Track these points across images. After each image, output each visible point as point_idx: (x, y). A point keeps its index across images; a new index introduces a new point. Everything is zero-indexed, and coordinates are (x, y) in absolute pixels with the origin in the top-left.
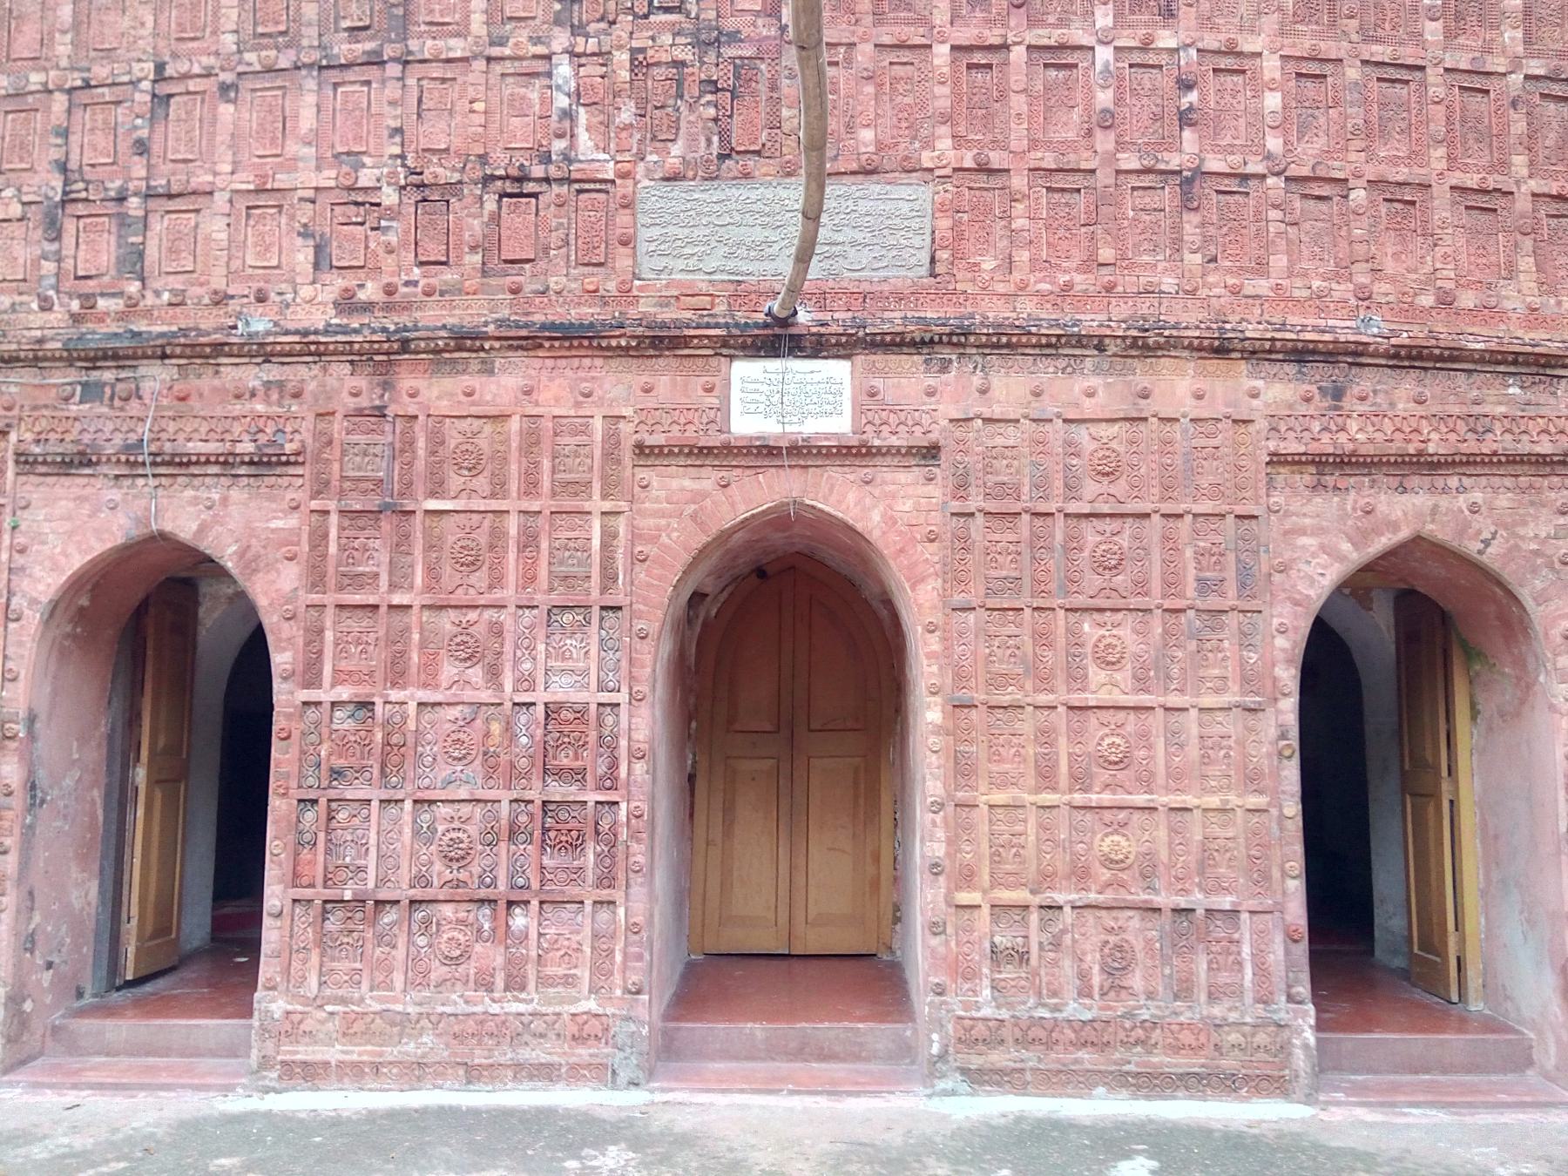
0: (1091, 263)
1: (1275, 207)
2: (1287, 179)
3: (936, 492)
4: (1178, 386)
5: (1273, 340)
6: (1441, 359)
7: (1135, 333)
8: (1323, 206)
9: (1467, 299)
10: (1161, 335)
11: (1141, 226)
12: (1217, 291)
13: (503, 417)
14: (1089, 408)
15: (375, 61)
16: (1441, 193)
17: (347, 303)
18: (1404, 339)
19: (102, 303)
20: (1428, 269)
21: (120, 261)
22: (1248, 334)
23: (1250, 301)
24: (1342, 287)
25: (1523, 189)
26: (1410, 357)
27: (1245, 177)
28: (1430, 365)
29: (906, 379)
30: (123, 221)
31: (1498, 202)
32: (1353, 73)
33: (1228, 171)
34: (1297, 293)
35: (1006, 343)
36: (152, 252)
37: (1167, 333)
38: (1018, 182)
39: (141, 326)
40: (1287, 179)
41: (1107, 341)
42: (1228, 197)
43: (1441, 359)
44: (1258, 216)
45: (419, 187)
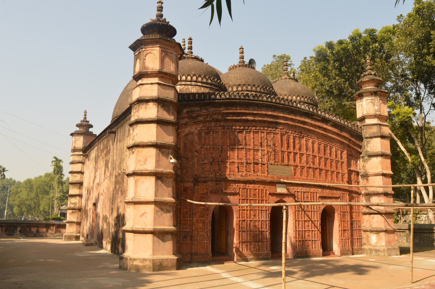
13: (256, 189)
14: (305, 191)
17: (242, 176)
19: (217, 174)
21: (219, 169)
36: (222, 169)
38: (299, 167)
39: (222, 177)
45: (247, 163)
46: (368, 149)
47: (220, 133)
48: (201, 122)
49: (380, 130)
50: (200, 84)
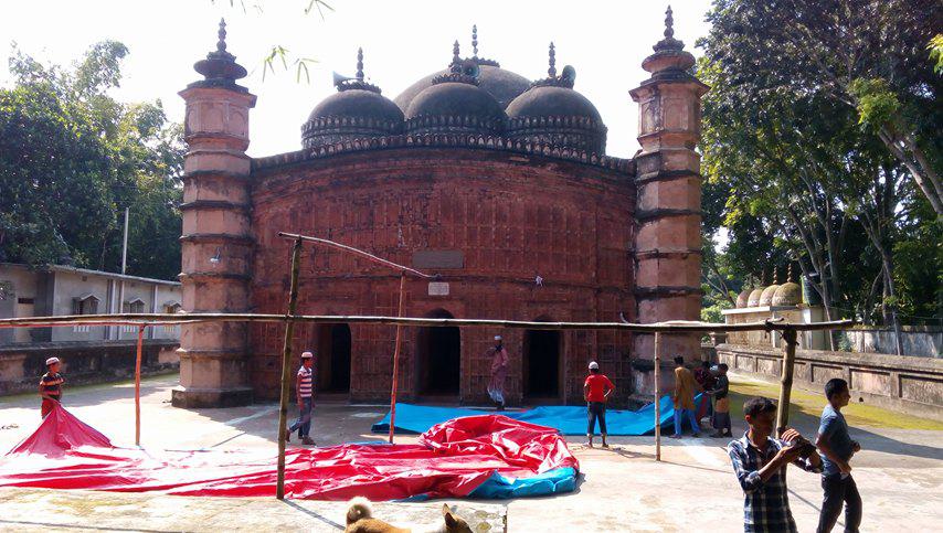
0: (490, 267)
3: (463, 306)
4: (505, 288)
15: (367, 229)
29: (458, 286)
30: (325, 258)
35: (476, 279)
46: (641, 206)
47: (328, 208)
48: (293, 195)
49: (661, 163)
50: (337, 130)
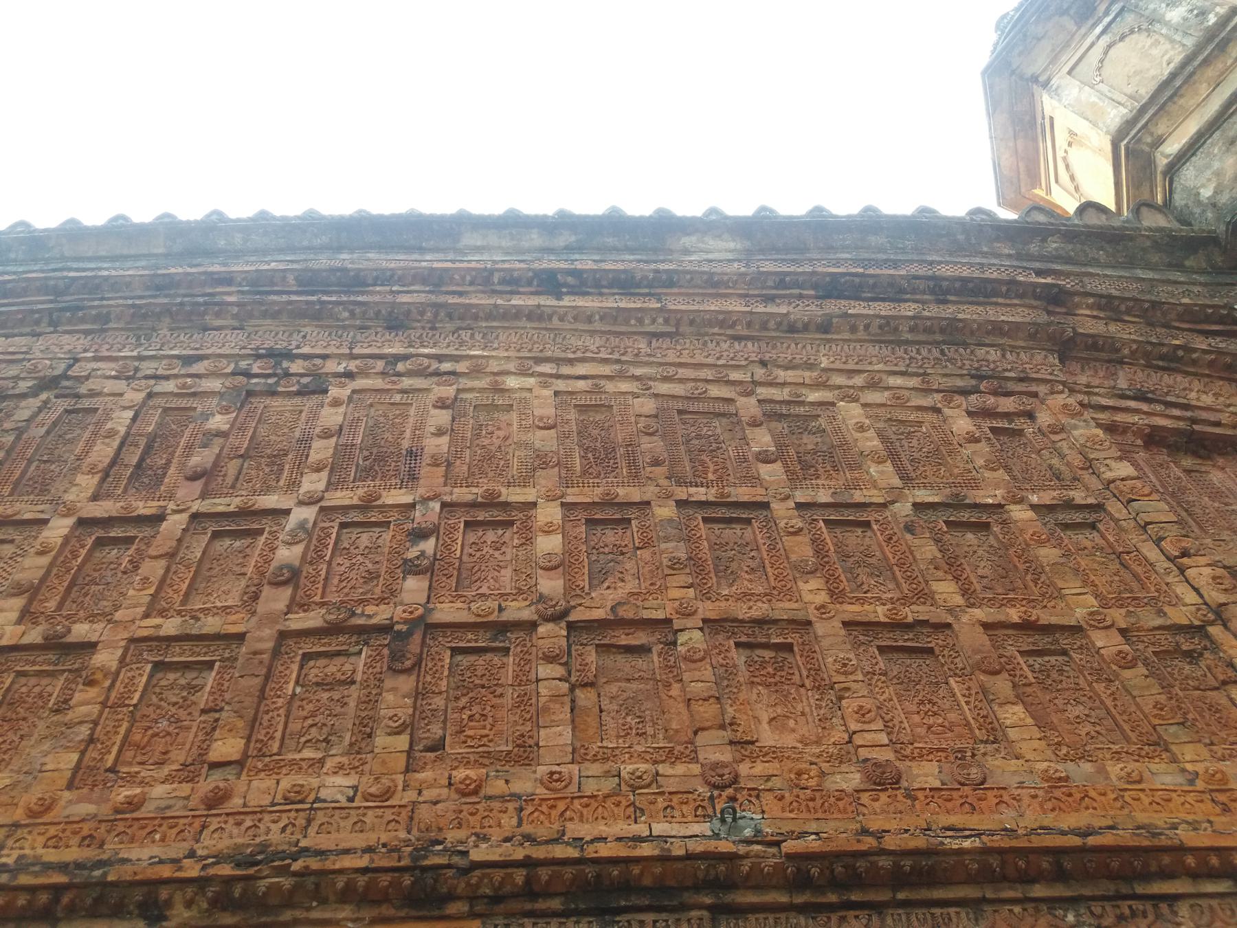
1: (550, 659)
2: (571, 626)
5: (528, 863)
6: (898, 879)
7: (226, 870)
8: (640, 663)
9: (926, 774)
10: (284, 871)
11: (310, 707)
12: (428, 794)
16: (828, 630)
18: (811, 844)
20: (839, 735)
22: (476, 855)
23: (496, 805)
24: (680, 769)
25: (965, 619)
26: (835, 884)
27: (503, 628)
28: (884, 896)
31: (934, 642)
32: (665, 511)
33: (472, 619)
34: (590, 787)
37: (296, 866)
40: (571, 626)
41: (164, 894)
42: (472, 658)
43: (898, 879)
44: (522, 678)
